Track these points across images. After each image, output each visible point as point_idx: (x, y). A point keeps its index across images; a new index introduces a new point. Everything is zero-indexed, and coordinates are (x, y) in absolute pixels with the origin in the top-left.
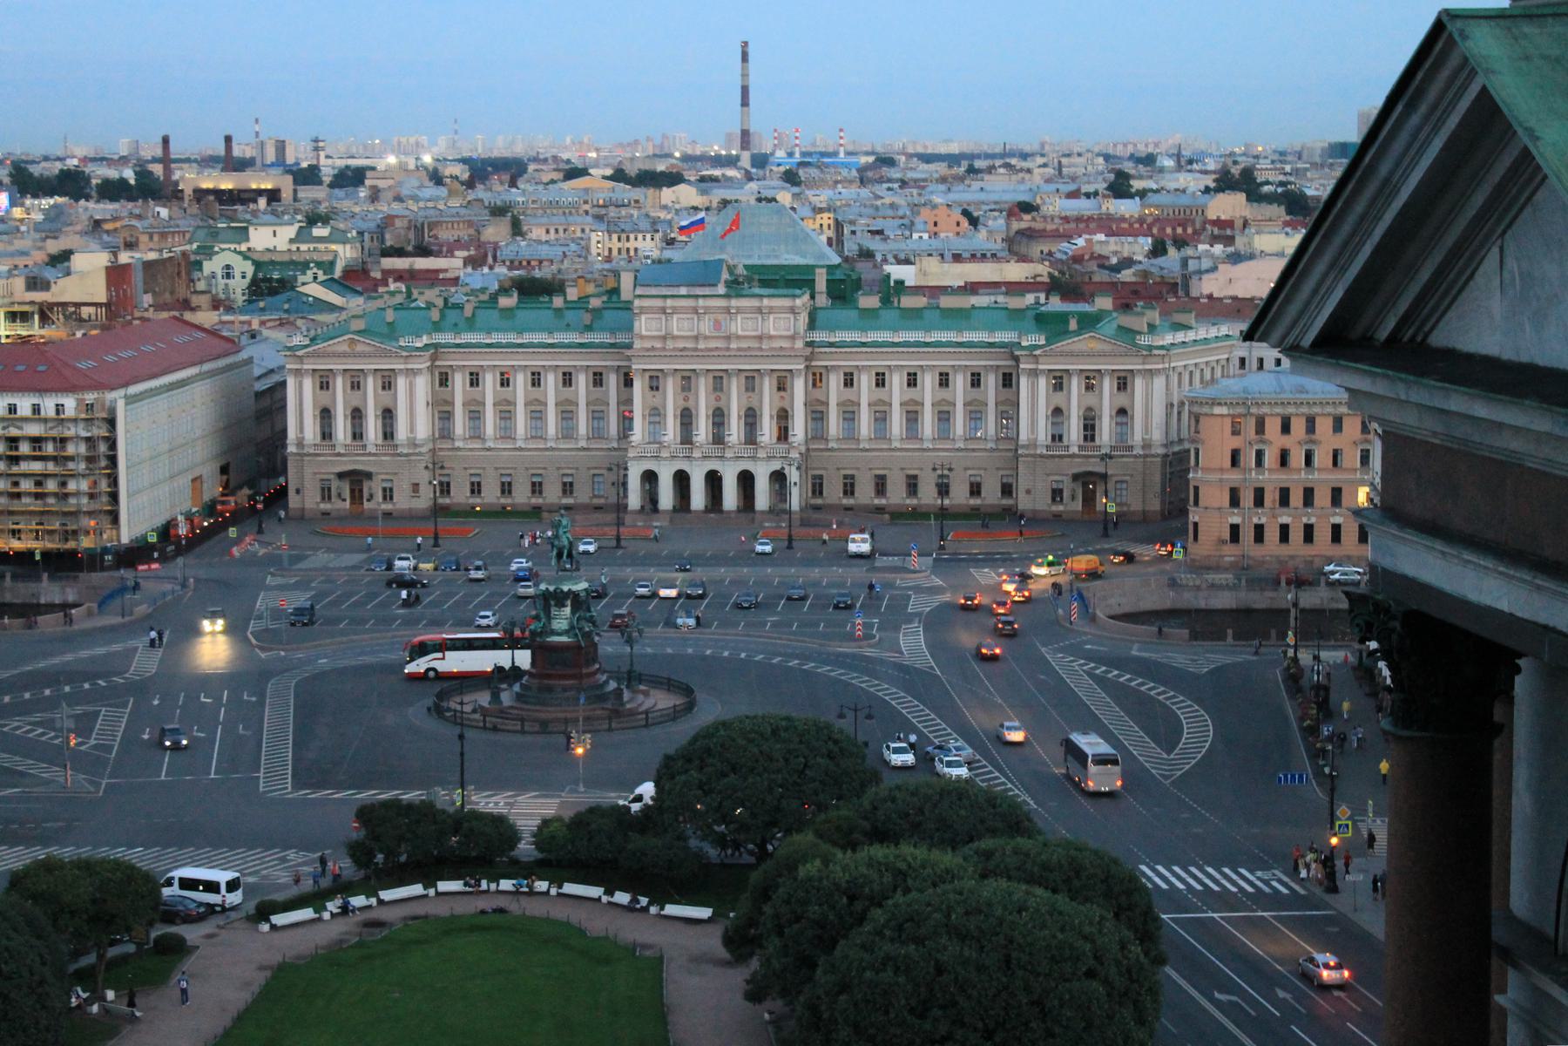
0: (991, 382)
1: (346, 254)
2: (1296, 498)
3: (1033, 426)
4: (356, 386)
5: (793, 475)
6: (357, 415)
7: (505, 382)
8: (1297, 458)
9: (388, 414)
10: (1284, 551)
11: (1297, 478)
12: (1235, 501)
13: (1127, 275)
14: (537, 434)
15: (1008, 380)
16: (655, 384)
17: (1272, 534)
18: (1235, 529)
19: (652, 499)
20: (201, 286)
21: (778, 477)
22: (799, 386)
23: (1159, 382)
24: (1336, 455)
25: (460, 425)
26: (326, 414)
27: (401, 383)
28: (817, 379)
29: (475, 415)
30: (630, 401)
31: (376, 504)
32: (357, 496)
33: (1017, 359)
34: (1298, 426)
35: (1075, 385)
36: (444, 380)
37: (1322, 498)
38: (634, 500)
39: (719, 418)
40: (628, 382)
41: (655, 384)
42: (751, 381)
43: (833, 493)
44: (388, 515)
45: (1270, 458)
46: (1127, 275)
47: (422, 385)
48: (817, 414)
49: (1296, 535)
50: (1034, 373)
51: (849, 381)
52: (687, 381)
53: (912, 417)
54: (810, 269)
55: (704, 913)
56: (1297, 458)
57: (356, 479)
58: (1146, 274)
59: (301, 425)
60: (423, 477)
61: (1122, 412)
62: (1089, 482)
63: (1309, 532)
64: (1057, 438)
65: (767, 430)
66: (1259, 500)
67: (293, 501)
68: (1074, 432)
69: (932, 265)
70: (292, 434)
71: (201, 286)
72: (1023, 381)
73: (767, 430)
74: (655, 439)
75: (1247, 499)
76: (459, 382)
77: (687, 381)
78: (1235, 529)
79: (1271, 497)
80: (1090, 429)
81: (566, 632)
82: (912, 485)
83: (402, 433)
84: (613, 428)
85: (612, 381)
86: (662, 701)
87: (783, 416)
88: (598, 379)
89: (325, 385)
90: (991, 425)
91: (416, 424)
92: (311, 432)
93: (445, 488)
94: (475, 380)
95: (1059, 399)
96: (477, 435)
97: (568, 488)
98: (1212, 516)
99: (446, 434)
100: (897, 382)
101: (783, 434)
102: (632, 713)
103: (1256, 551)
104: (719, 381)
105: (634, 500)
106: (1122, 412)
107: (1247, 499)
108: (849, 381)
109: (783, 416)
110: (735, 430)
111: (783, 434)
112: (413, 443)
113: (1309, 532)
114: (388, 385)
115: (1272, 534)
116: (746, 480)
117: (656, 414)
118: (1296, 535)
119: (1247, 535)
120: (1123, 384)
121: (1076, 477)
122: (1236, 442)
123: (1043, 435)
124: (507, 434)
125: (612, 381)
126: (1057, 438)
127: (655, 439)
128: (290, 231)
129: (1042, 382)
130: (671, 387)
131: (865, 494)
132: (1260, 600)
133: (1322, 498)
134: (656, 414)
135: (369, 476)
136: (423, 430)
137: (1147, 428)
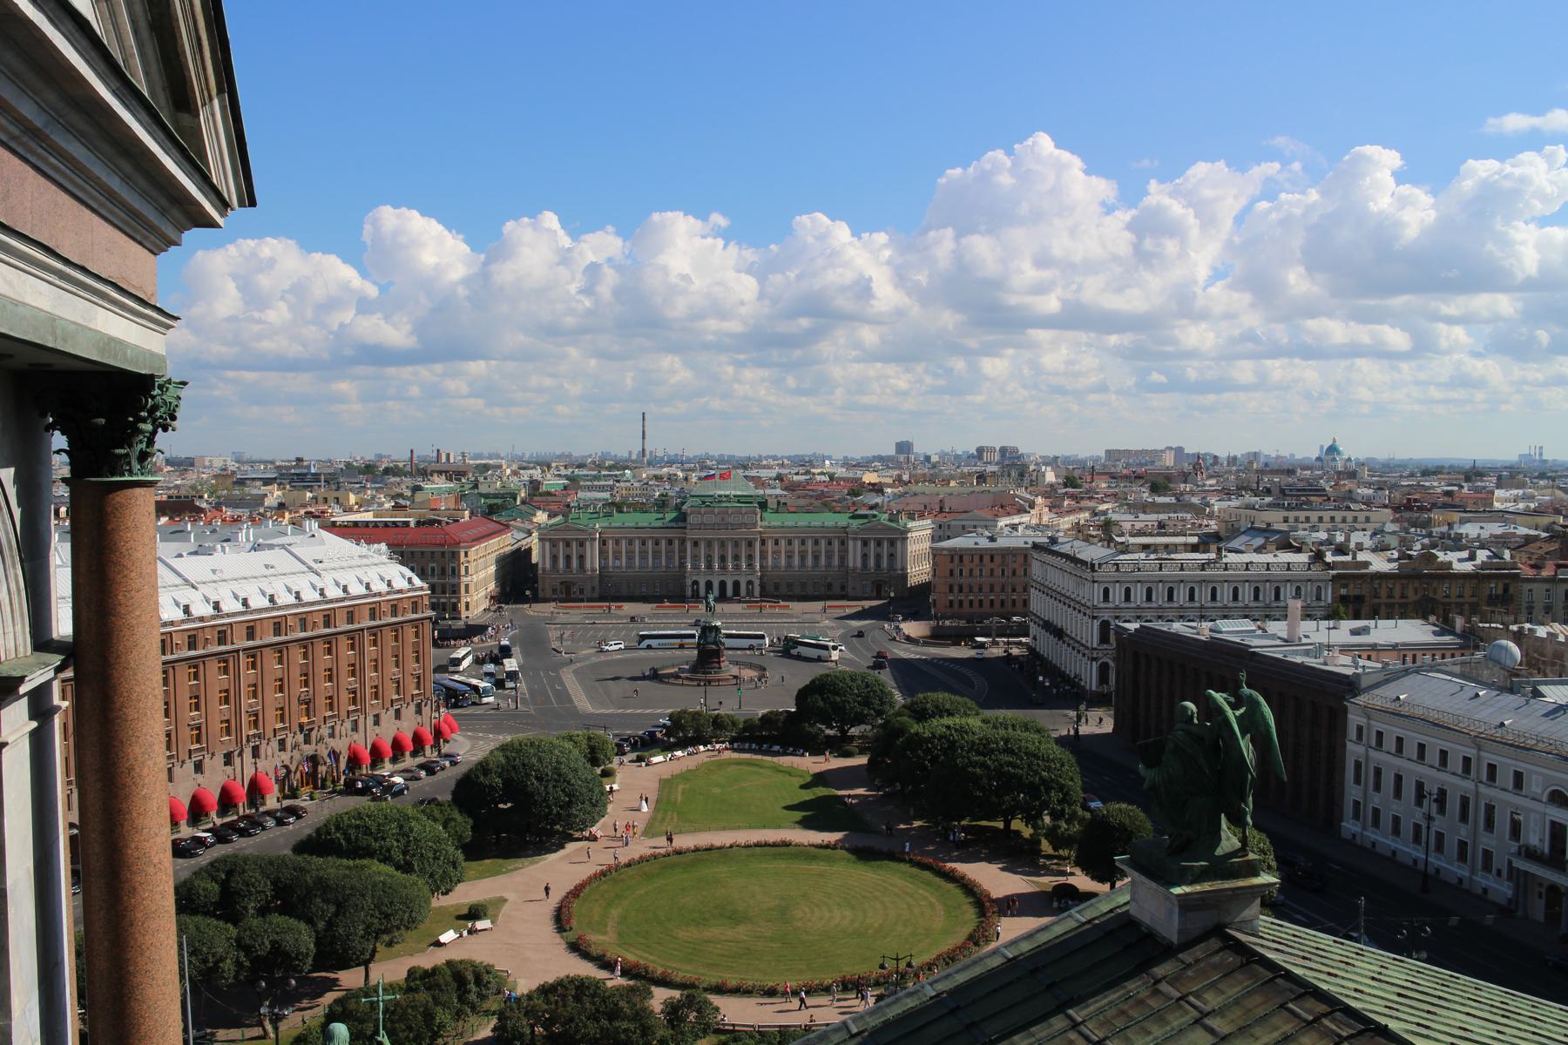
0: (836, 543)
2: (976, 589)
3: (854, 559)
6: (568, 558)
9: (582, 558)
12: (951, 590)
16: (696, 544)
17: (966, 604)
21: (750, 583)
22: (758, 544)
26: (555, 558)
28: (763, 542)
32: (568, 592)
37: (986, 589)
38: (689, 592)
40: (683, 542)
41: (696, 544)
43: (770, 589)
48: (763, 556)
49: (976, 604)
51: (777, 543)
64: (865, 564)
67: (541, 594)
68: (872, 562)
72: (851, 543)
75: (956, 589)
76: (610, 543)
81: (715, 643)
83: (588, 566)
88: (670, 542)
90: (836, 561)
92: (548, 566)
101: (750, 566)
105: (689, 592)
107: (956, 589)
109: (750, 557)
111: (750, 566)
114: (581, 544)
115: (966, 604)
116: (736, 585)
117: (695, 558)
118: (976, 604)
119: (956, 605)
120: (892, 543)
122: (951, 566)
123: (859, 564)
130: (702, 545)
131: (784, 590)
133: (986, 589)
134: (695, 558)
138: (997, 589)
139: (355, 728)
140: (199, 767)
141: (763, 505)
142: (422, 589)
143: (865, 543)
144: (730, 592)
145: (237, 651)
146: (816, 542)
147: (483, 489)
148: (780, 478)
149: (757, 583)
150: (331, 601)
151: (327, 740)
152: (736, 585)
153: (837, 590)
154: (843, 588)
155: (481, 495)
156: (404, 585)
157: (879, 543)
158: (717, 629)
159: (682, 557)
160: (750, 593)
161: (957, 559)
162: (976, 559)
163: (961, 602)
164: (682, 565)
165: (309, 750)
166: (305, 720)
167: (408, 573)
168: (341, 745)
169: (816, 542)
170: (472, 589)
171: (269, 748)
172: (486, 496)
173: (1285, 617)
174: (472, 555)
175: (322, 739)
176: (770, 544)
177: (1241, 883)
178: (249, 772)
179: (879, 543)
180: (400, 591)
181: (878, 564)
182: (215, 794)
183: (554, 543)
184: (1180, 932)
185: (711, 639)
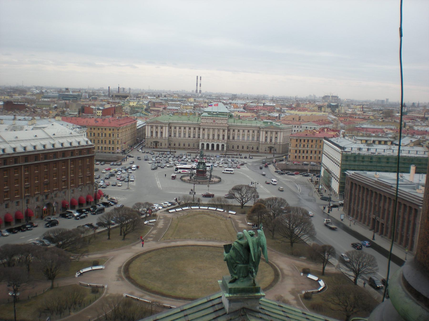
0: (256, 132)
1: (145, 107)
2: (305, 152)
3: (262, 139)
4: (157, 128)
5: (225, 145)
6: (157, 132)
7: (180, 128)
8: (306, 146)
9: (162, 132)
10: (303, 160)
11: (306, 149)
13: (265, 116)
14: (185, 137)
15: (259, 132)
16: (204, 130)
17: (301, 157)
18: (296, 156)
19: (203, 147)
20: (123, 111)
21: (223, 145)
23: (282, 133)
24: (312, 145)
25: (173, 135)
26: (152, 132)
27: (164, 128)
28: (229, 130)
29: (175, 134)
30: (200, 132)
31: (160, 146)
33: (260, 128)
34: (306, 141)
35: (269, 133)
36: (170, 128)
37: (309, 152)
38: (200, 148)
39: (214, 135)
40: (199, 129)
41: (204, 130)
42: (219, 130)
43: (231, 147)
44: (161, 148)
45: (302, 146)
46: (265, 116)
47: (167, 128)
50: (263, 131)
51: (234, 131)
52: (209, 129)
53: (243, 137)
54: (227, 113)
55: (234, 213)
56: (306, 146)
57: (156, 143)
58: (269, 116)
59: (148, 133)
60: (167, 142)
61: (276, 137)
62: (271, 148)
63: (307, 157)
64: (266, 140)
65: (221, 137)
66: (300, 152)
69: (237, 113)
70: (146, 135)
71: (123, 111)
72: (261, 132)
73: (221, 137)
74: (203, 138)
75: (298, 151)
76: (173, 128)
77: (209, 129)
78: (296, 156)
79: (301, 152)
80: (271, 141)
82: (243, 147)
83: (164, 136)
84: (197, 136)
85: (197, 129)
86: (217, 180)
87: (224, 136)
88: (195, 129)
89: (152, 128)
90: (255, 139)
91: (166, 134)
92: (149, 135)
93: (170, 145)
94: (175, 128)
95: (266, 135)
96: (175, 136)
97: (189, 145)
98: (292, 154)
99: (170, 136)
100: (241, 131)
101: (223, 139)
102: (212, 181)
103: (299, 160)
104: (214, 129)
105: (200, 148)
106: (276, 137)
107: (298, 151)
108: (234, 131)
109: (224, 136)
110: (216, 137)
111: (223, 139)
112: (165, 137)
113: (307, 157)
114: (162, 128)
115: (301, 157)
116: (218, 146)
117: (204, 134)
119: (298, 157)
120: (277, 133)
121: (269, 147)
122: (297, 143)
123: (264, 140)
124: (180, 136)
125: (197, 129)
126: (266, 140)
127: (203, 138)
128: (136, 103)
129: (264, 132)
130: (206, 130)
132: (300, 168)
133: (309, 152)
134: (204, 134)
135: (158, 142)
136: (167, 136)
137: (280, 140)
138: (313, 152)
139: (65, 195)
140: (7, 206)
141: (231, 116)
142: (91, 145)
143: (266, 132)
144: (215, 148)
145: (21, 166)
146: (249, 131)
147: (131, 104)
148: (245, 105)
149: (225, 145)
150: (57, 149)
151: (54, 198)
152: (218, 146)
153: (255, 149)
154: (257, 149)
155: (130, 106)
156: (85, 144)
157: (272, 132)
158: (204, 164)
159: (199, 135)
160: (223, 148)
161: (299, 141)
162: (306, 141)
163: (299, 156)
164: (199, 137)
165: (47, 201)
166: (46, 191)
167: (87, 139)
168: (60, 200)
169: (249, 131)
170: (120, 142)
171: (32, 200)
172: (132, 108)
173: (409, 172)
174: (120, 131)
175: (52, 197)
176: (231, 131)
177: (251, 295)
178: (25, 208)
179: (272, 132)
180: (83, 146)
181: (271, 141)
182: (13, 215)
183: (152, 127)
184: (229, 309)
185: (201, 167)
